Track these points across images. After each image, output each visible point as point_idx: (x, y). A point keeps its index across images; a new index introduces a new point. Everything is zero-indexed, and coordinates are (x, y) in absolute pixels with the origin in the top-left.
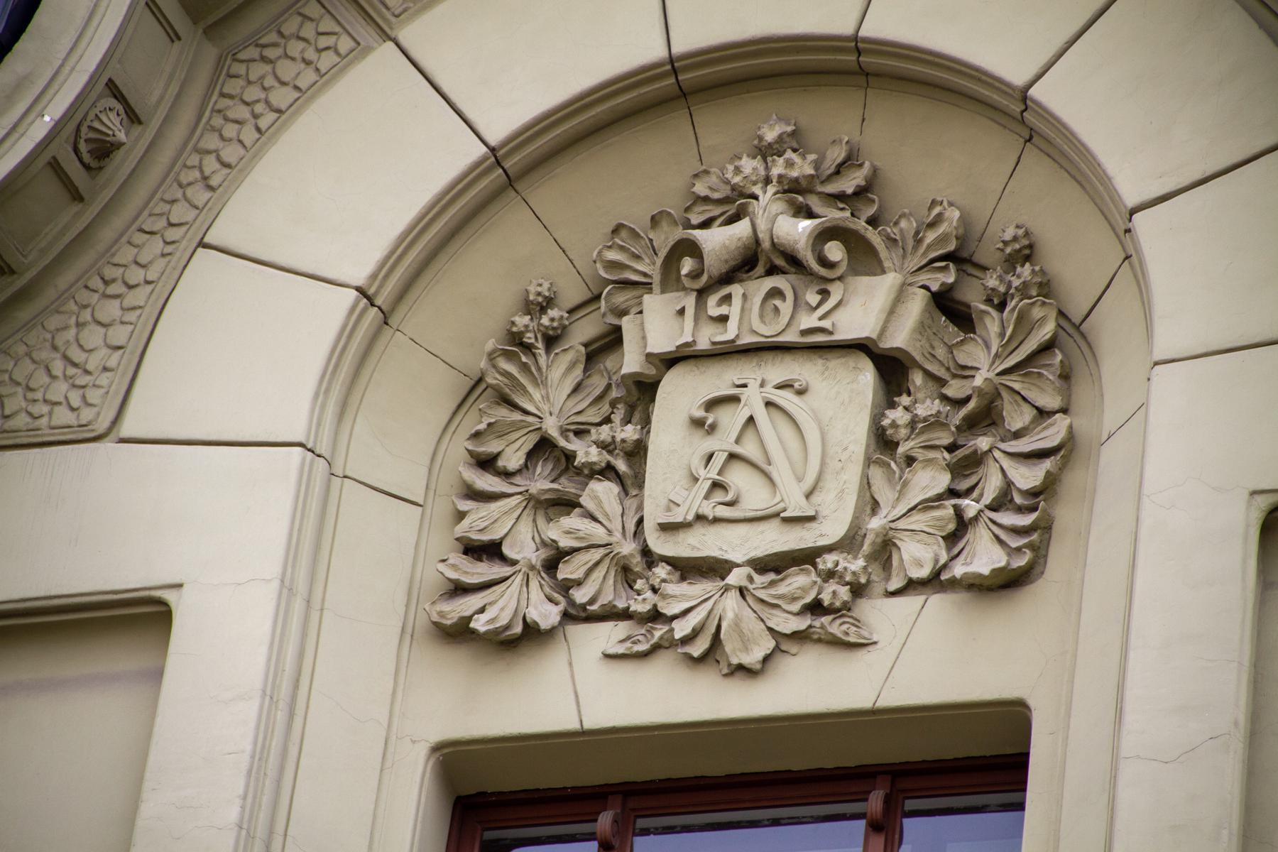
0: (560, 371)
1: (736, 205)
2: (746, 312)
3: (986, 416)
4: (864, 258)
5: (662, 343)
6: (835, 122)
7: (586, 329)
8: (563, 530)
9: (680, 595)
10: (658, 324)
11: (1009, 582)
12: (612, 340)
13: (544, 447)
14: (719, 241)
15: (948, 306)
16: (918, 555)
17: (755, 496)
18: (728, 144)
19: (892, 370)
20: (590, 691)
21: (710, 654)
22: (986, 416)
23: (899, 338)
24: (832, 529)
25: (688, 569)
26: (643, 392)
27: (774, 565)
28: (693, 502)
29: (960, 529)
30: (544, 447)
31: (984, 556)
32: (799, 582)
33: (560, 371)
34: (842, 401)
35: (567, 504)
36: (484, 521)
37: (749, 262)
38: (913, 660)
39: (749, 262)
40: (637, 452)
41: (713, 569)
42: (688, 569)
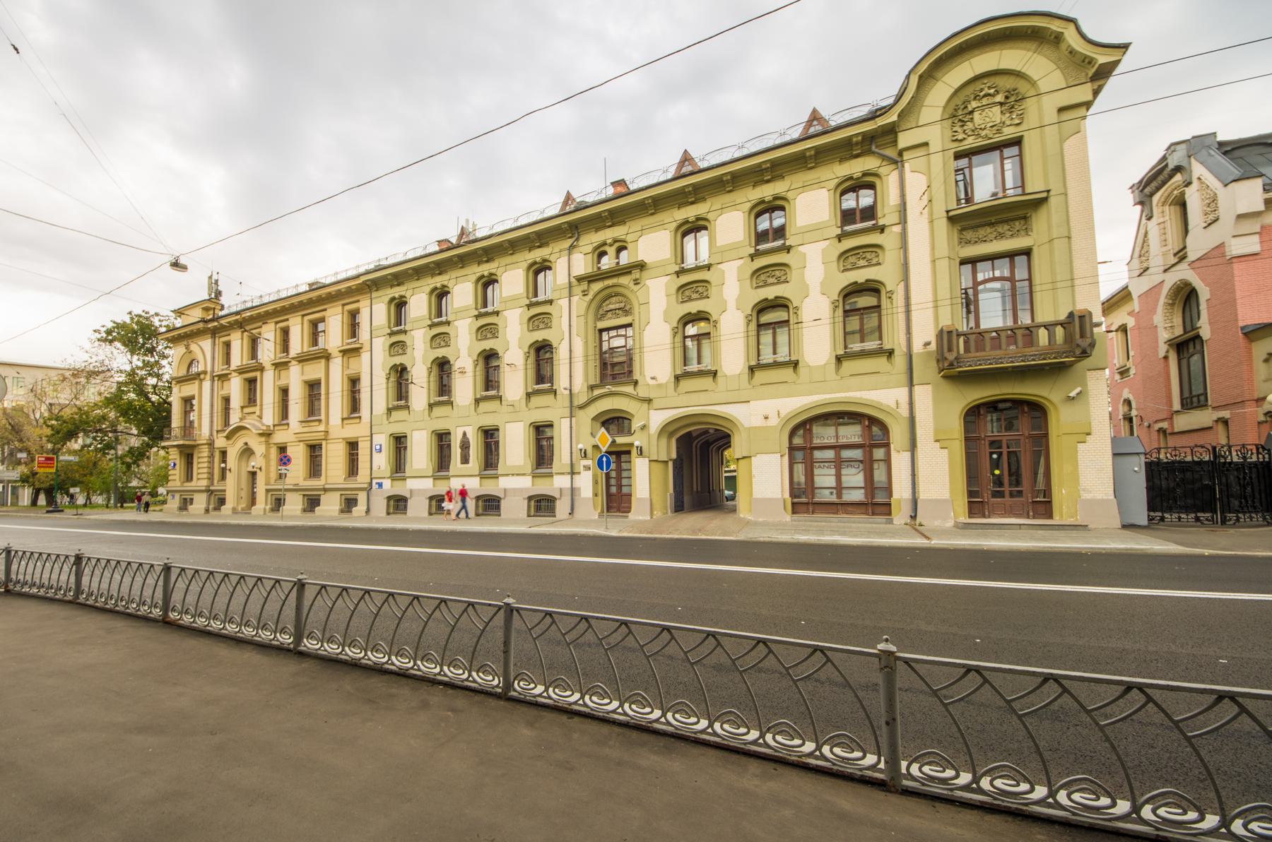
0: (960, 112)
1: (982, 90)
2: (985, 101)
10: (974, 104)
16: (1008, 122)
18: (978, 85)
20: (971, 142)
26: (972, 112)
37: (985, 96)
38: (1009, 132)
39: (985, 96)
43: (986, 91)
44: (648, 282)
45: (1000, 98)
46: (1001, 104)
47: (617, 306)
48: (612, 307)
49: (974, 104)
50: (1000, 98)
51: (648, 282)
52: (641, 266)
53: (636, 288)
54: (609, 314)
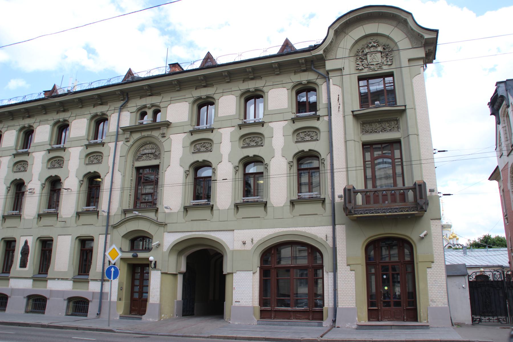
0: (360, 54)
1: (370, 43)
2: (372, 49)
3: (387, 55)
4: (379, 46)
5: (367, 51)
6: (376, 38)
7: (361, 51)
8: (363, 63)
9: (371, 66)
10: (367, 50)
11: (391, 64)
12: (363, 51)
13: (360, 58)
14: (370, 45)
15: (384, 49)
16: (385, 63)
17: (375, 60)
18: (369, 40)
19: (381, 52)
20: (366, 72)
21: (374, 70)
22: (387, 55)
23: (382, 50)
24: (380, 62)
25: (371, 65)
26: (366, 55)
27: (377, 64)
28: (371, 61)
29: (387, 61)
30: (360, 58)
31: (390, 63)
32: (378, 65)
33: (360, 54)
34: (379, 55)
35: (362, 61)
36: (358, 63)
37: (372, 46)
38: (386, 69)
39: (372, 46)
40: (367, 58)
41: (373, 65)
42: (371, 65)
43: (373, 44)
44: (172, 137)
45: (380, 49)
46: (381, 52)
47: (150, 151)
48: (146, 151)
49: (367, 50)
50: (380, 49)
51: (172, 137)
52: (167, 124)
53: (163, 140)
54: (144, 157)
